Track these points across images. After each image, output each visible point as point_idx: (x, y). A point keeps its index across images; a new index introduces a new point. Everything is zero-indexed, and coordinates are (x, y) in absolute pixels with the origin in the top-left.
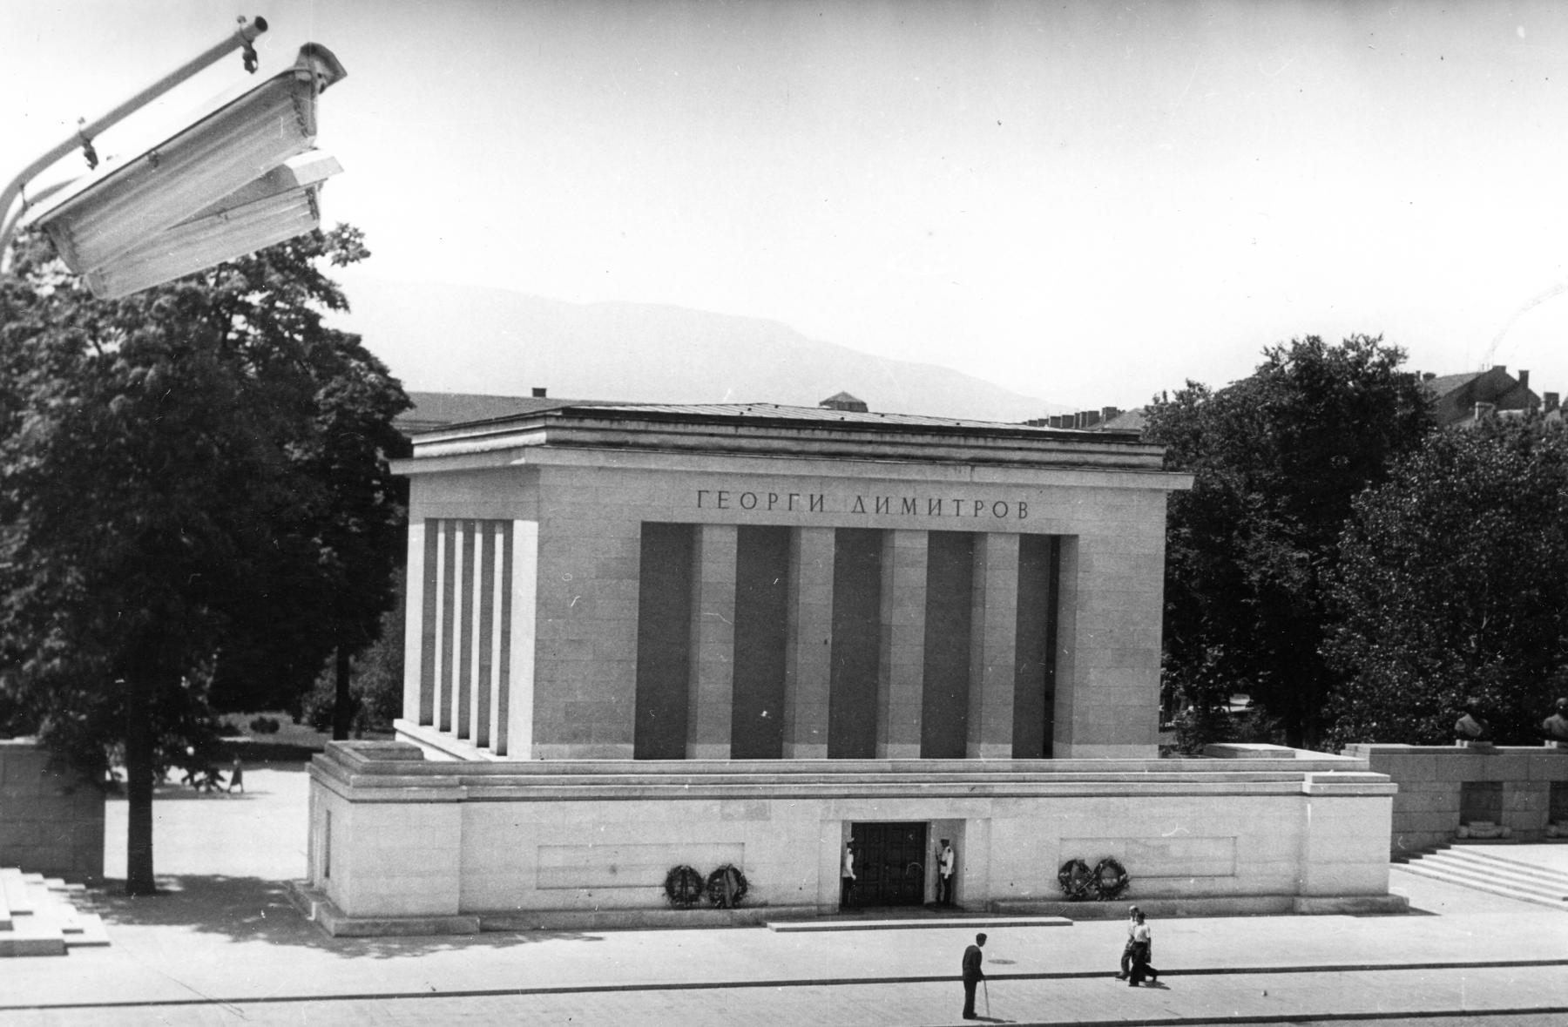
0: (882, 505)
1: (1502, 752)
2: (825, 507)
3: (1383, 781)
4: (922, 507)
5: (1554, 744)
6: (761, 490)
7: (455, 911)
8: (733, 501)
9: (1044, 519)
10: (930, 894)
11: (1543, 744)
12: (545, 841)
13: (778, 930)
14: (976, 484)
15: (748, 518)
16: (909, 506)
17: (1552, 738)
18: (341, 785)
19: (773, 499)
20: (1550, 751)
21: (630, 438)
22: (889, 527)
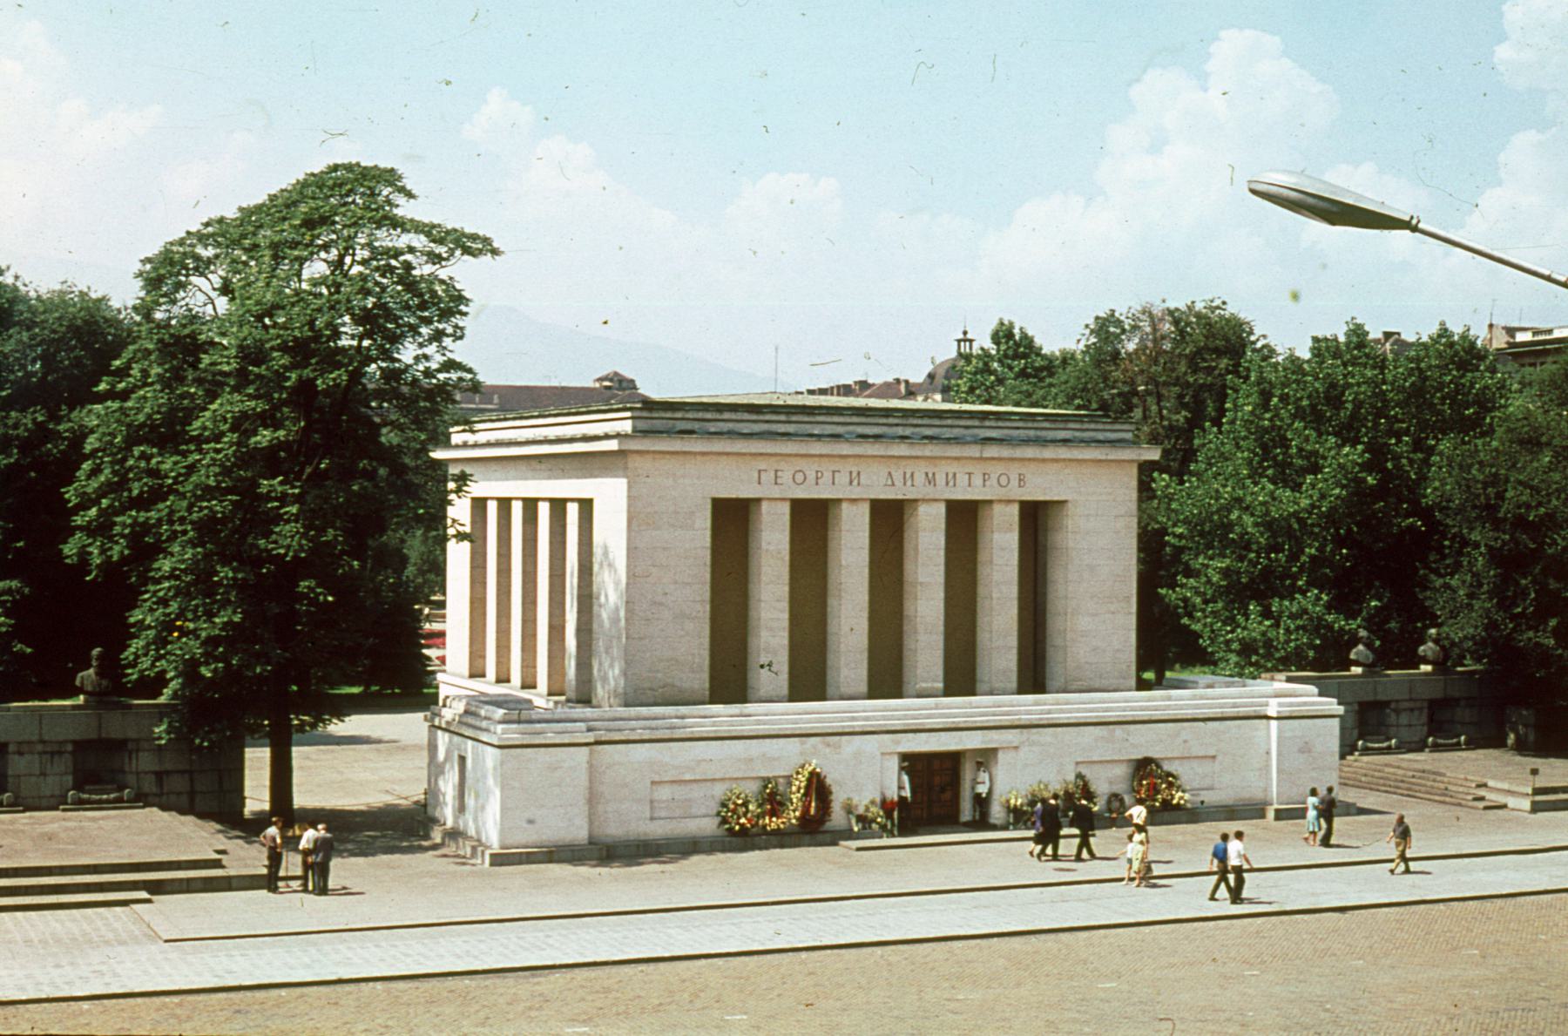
0: (909, 478)
1: (1388, 676)
2: (862, 481)
3: (1331, 704)
4: (941, 479)
5: (1429, 668)
6: (810, 468)
7: (586, 842)
8: (786, 477)
9: (1036, 491)
10: (967, 812)
11: (1418, 668)
12: (657, 778)
13: (859, 849)
14: (987, 459)
15: (801, 494)
16: (931, 480)
17: (1427, 662)
18: (485, 733)
19: (768, 477)
20: (1426, 674)
21: (696, 426)
22: (1056, 498)
